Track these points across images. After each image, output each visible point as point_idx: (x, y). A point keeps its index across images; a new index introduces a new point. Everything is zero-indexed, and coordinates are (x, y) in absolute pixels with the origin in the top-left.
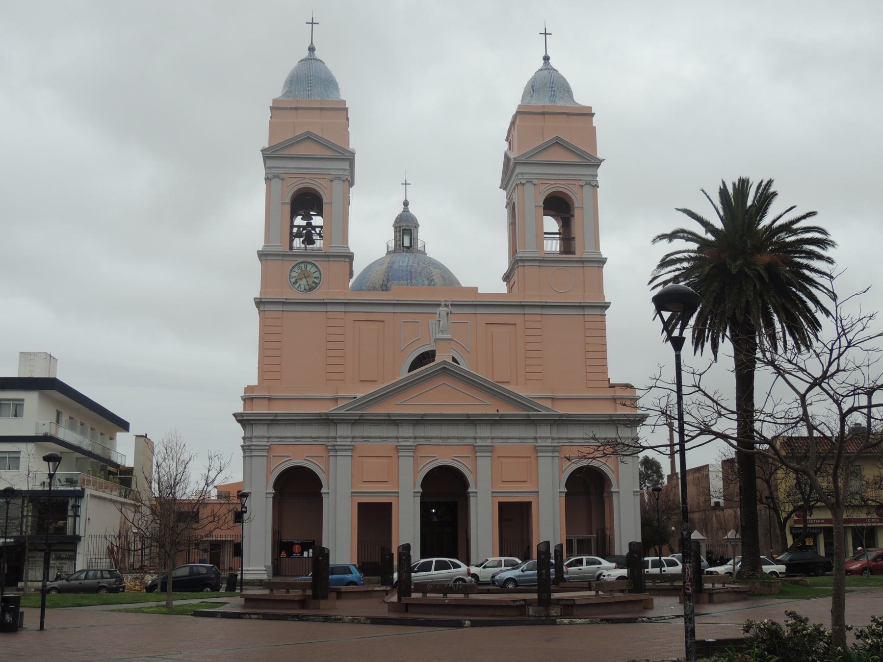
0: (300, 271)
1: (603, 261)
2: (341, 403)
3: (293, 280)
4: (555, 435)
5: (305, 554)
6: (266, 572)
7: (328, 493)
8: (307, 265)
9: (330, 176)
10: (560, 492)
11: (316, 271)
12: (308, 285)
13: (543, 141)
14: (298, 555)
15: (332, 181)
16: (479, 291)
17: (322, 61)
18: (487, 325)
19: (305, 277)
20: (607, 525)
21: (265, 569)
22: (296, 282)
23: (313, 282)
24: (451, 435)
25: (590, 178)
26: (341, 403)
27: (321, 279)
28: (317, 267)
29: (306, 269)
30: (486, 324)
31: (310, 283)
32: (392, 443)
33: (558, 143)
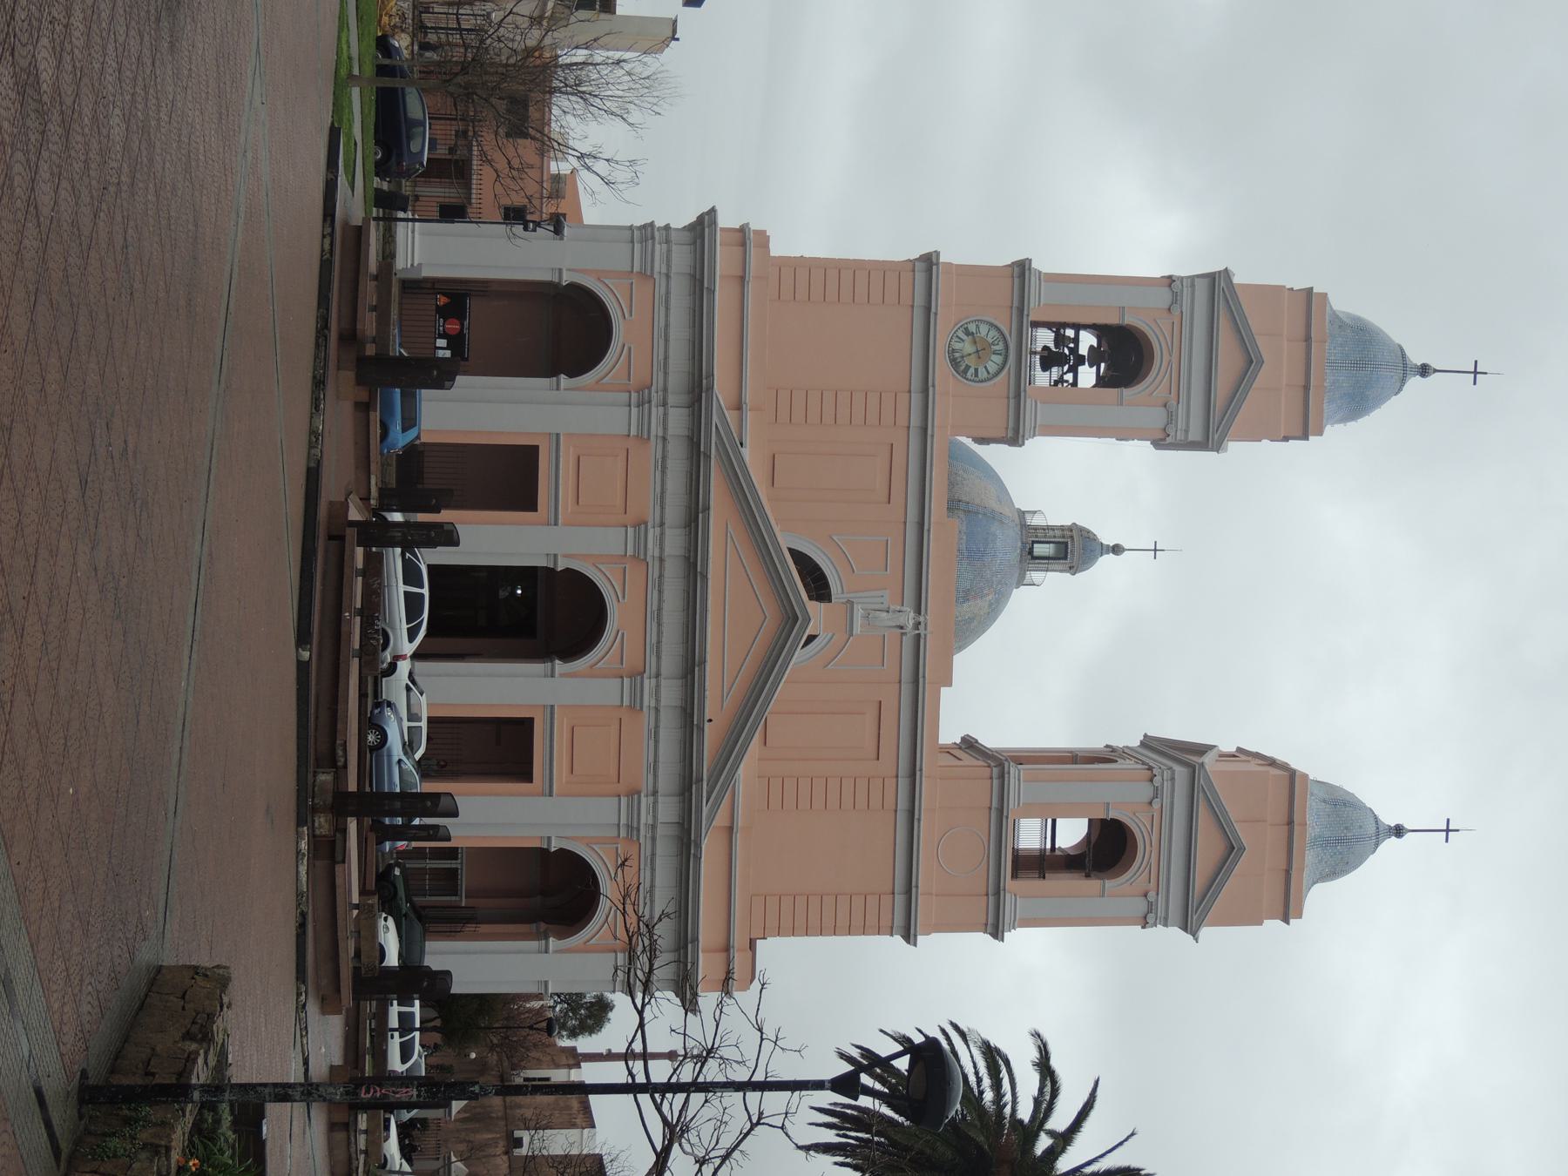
0: (990, 341)
1: (997, 934)
2: (731, 416)
3: (972, 328)
4: (660, 831)
5: (442, 343)
6: (409, 266)
7: (558, 389)
8: (1000, 354)
9: (1175, 404)
10: (549, 839)
11: (988, 373)
12: (963, 357)
13: (1236, 822)
14: (441, 329)
15: (1165, 406)
16: (943, 690)
17: (1400, 389)
18: (877, 705)
19: (978, 351)
20: (484, 928)
21: (415, 265)
22: (968, 333)
23: (968, 367)
24: (665, 629)
25: (1161, 913)
26: (731, 416)
27: (973, 381)
28: (997, 374)
30: (880, 702)
31: (967, 361)
32: (652, 516)
33: (1232, 850)
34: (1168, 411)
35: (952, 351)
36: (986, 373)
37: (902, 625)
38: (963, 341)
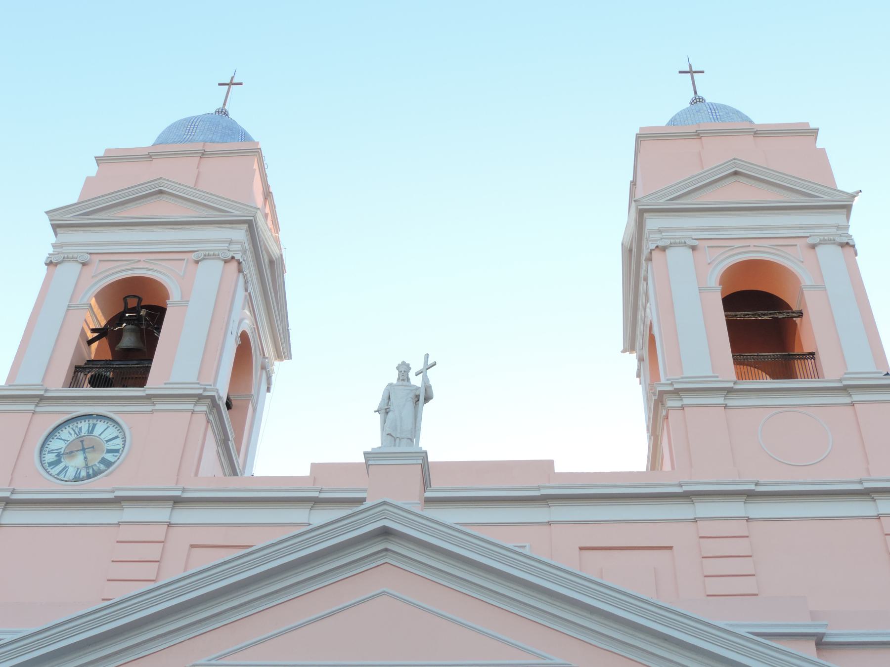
0: (74, 437)
3: (50, 457)
8: (94, 425)
13: (703, 169)
16: (558, 469)
19: (84, 450)
29: (92, 431)
30: (581, 549)
34: (203, 259)
35: (76, 479)
36: (118, 439)
37: (412, 395)
38: (66, 467)
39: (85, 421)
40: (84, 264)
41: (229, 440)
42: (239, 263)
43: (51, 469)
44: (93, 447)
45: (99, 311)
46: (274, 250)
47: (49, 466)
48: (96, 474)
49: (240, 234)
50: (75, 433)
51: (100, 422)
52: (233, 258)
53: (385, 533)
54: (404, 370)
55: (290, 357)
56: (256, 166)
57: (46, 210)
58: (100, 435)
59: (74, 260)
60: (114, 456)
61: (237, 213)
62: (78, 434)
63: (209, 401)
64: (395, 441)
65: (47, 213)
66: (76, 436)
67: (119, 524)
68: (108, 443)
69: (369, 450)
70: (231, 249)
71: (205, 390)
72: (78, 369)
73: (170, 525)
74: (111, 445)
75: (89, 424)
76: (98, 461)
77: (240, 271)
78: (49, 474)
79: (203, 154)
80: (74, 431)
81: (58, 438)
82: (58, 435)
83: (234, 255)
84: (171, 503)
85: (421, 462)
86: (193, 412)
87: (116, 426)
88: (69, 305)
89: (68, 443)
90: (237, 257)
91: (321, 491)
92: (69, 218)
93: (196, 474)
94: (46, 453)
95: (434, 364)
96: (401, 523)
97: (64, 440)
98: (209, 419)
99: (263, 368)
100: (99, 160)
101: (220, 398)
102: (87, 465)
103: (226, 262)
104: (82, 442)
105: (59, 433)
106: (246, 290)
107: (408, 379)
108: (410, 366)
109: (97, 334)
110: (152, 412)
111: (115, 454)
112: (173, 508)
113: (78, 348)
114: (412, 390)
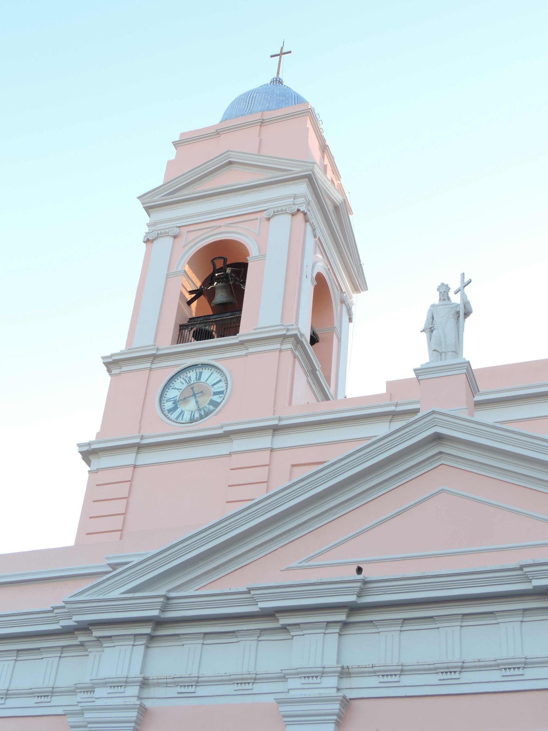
0: (185, 385)
3: (168, 405)
8: (201, 373)
11: (220, 381)
19: (194, 395)
23: (212, 403)
29: (200, 379)
34: (274, 216)
35: (192, 421)
37: (453, 312)
38: (182, 412)
39: (193, 371)
40: (175, 237)
41: (316, 370)
42: (305, 214)
43: (171, 415)
44: (202, 392)
45: (193, 274)
46: (337, 197)
47: (168, 413)
48: (207, 414)
49: (302, 188)
50: (186, 382)
51: (205, 369)
52: (298, 210)
53: (438, 438)
54: (444, 291)
55: (366, 289)
56: (309, 125)
57: (138, 196)
58: (206, 381)
59: (166, 234)
60: (219, 397)
61: (297, 171)
62: (188, 382)
63: (292, 339)
64: (441, 355)
65: (139, 198)
66: (187, 384)
67: (230, 454)
68: (214, 387)
69: (418, 366)
70: (296, 203)
71: (288, 330)
72: (182, 327)
73: (272, 450)
74: (217, 389)
75: (196, 373)
76: (208, 403)
77: (307, 221)
78: (169, 419)
79: (262, 123)
80: (185, 380)
81: (173, 388)
82: (172, 385)
83: (299, 208)
84: (271, 431)
85: (465, 371)
86: (281, 351)
87: (218, 371)
88: (167, 274)
89: (181, 391)
90: (302, 209)
91: (397, 405)
92: (158, 199)
93: (290, 403)
94: (165, 401)
95: (470, 281)
96: (450, 428)
97: (178, 389)
98: (295, 355)
99: (343, 302)
100: (176, 144)
101: (302, 335)
102: (198, 407)
103: (293, 215)
104: (192, 388)
105: (173, 384)
106: (315, 236)
107: (449, 299)
108: (449, 286)
109: (194, 295)
110: (246, 355)
111: (221, 395)
112: (273, 436)
113: (179, 309)
114: (452, 308)
